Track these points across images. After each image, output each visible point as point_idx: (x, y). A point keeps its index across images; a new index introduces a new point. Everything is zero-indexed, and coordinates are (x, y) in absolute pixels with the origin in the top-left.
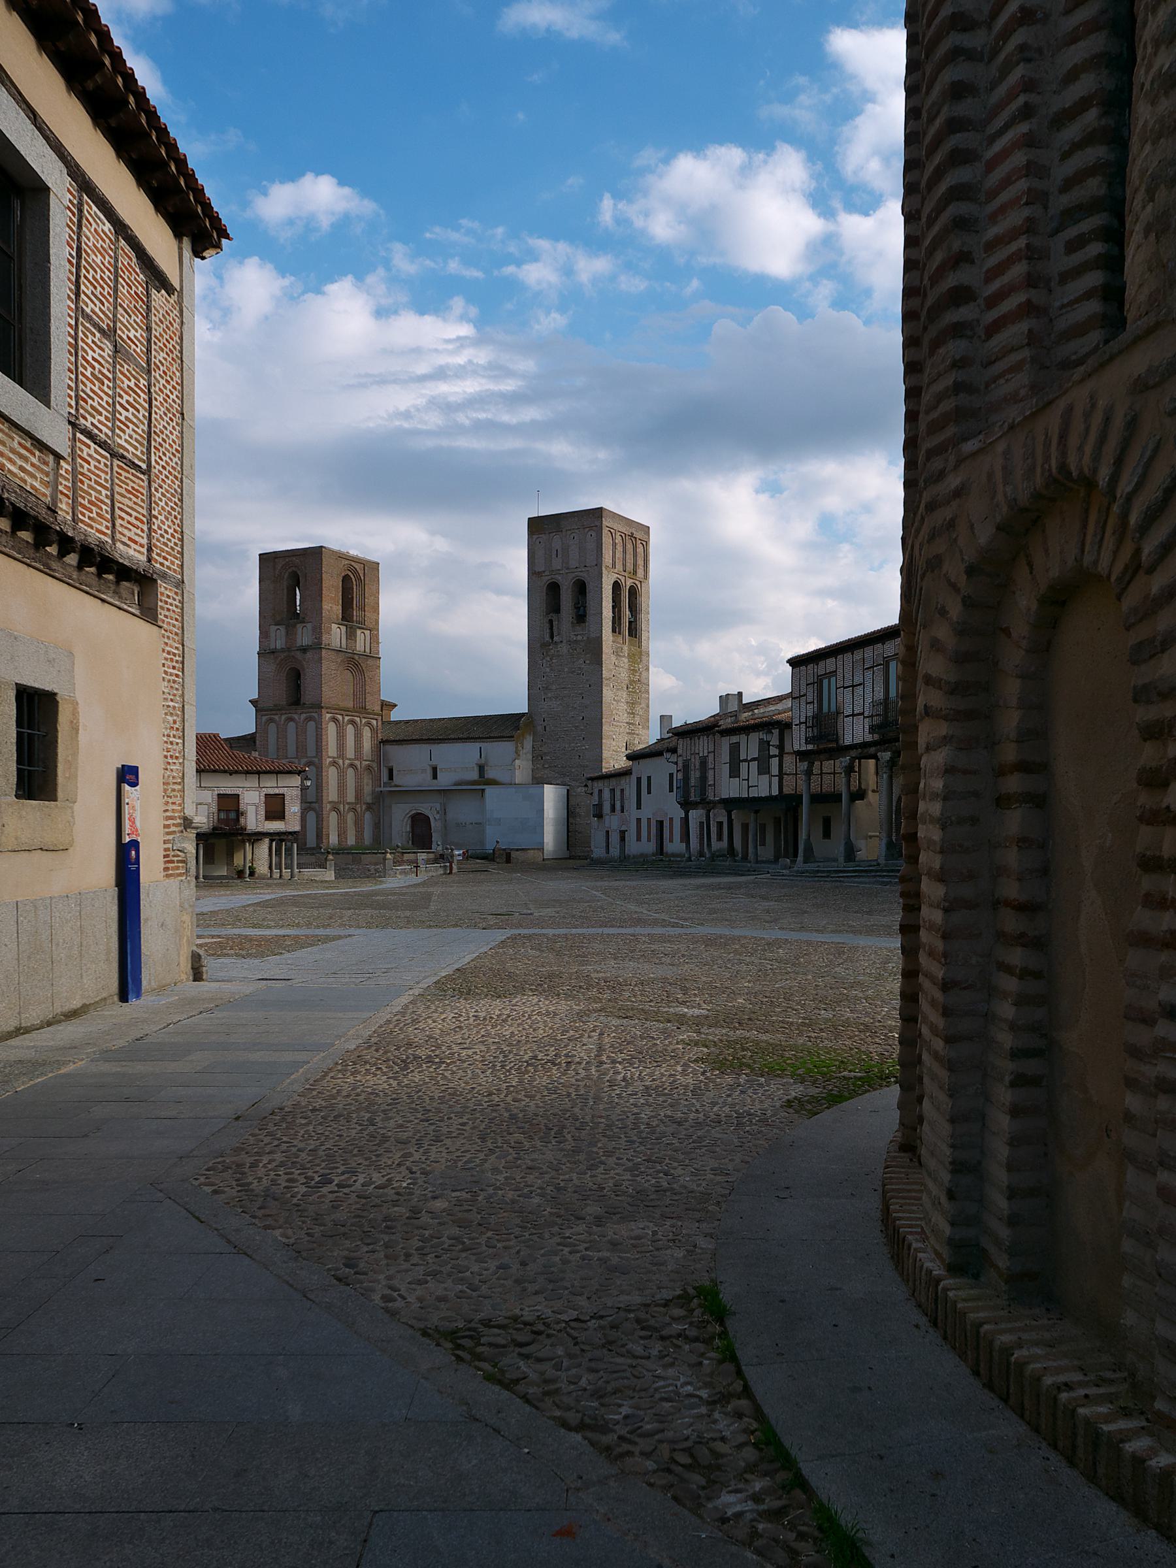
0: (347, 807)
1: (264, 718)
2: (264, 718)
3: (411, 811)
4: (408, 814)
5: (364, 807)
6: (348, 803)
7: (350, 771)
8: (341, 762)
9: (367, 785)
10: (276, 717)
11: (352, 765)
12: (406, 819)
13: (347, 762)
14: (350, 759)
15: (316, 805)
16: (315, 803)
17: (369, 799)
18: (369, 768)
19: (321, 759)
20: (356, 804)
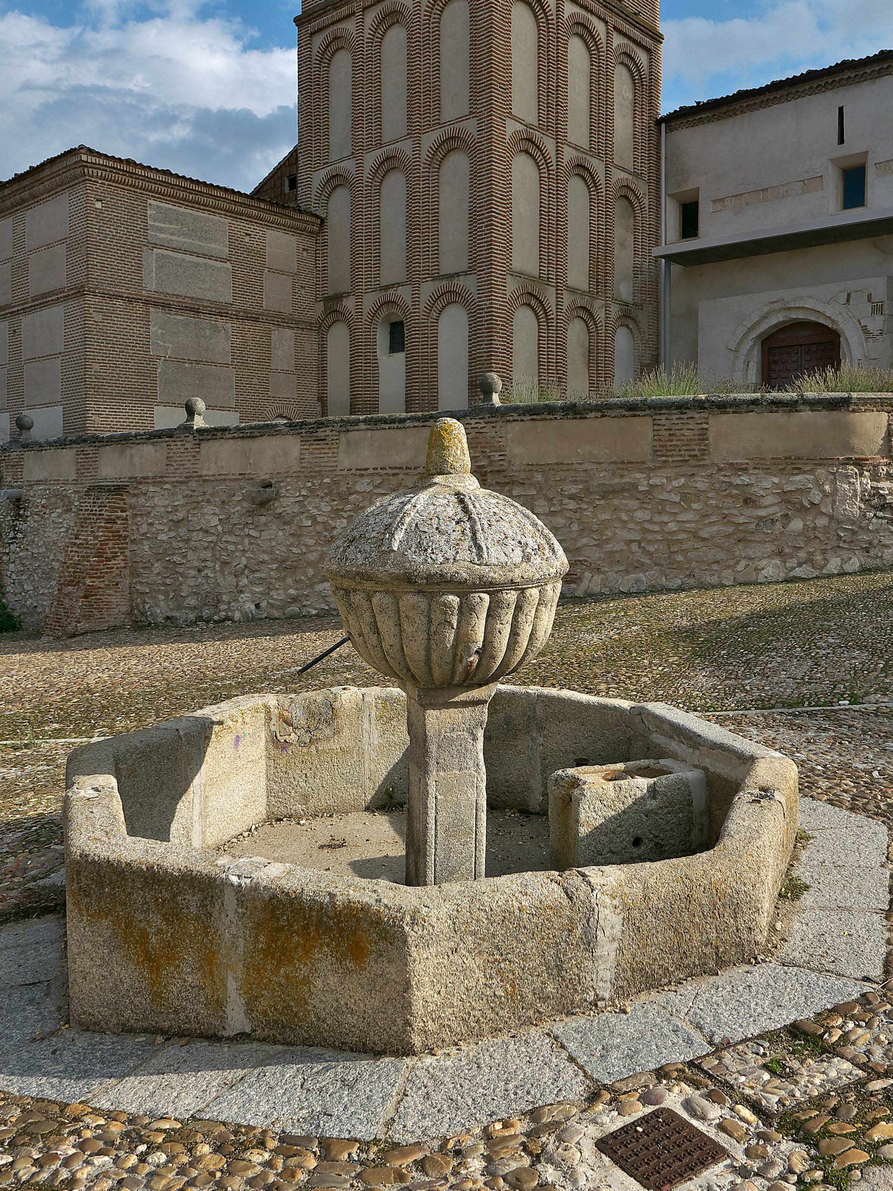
0: (567, 299)
1: (319, 41)
2: (319, 41)
3: (764, 318)
4: (750, 329)
5: (614, 309)
6: (573, 291)
7: (576, 188)
8: (549, 145)
9: (622, 245)
10: (350, 26)
11: (582, 170)
12: (748, 344)
13: (569, 154)
14: (576, 148)
15: (468, 283)
16: (466, 273)
17: (624, 290)
18: (627, 194)
19: (486, 128)
20: (593, 295)
